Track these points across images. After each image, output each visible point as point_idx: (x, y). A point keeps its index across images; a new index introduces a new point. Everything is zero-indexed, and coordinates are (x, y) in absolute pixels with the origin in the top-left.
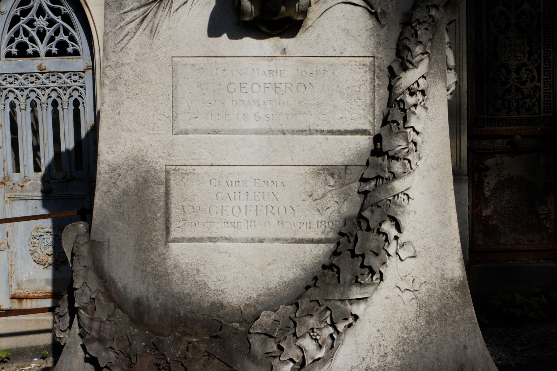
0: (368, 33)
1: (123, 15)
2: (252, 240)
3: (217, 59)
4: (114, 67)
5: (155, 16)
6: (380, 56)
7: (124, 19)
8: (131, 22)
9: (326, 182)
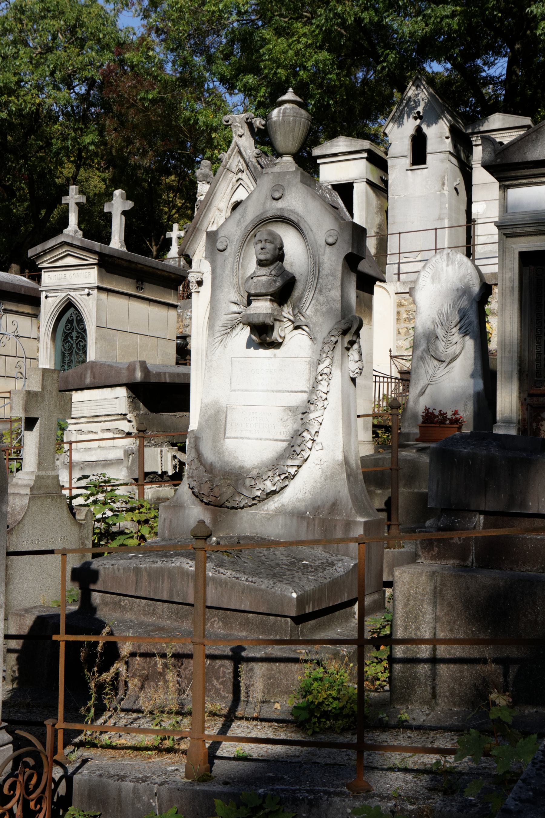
2: (257, 439)
9: (288, 414)
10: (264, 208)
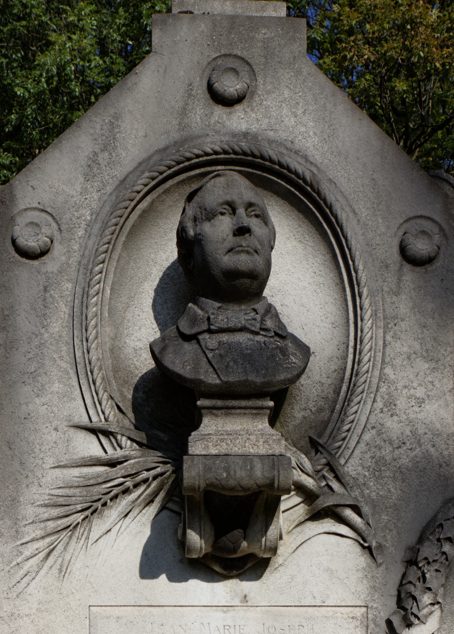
0: (360, 575)
1: (20, 548)
3: (152, 608)
4: (7, 619)
5: (65, 549)
6: (375, 606)
7: (21, 553)
8: (31, 557)
10: (182, 127)
